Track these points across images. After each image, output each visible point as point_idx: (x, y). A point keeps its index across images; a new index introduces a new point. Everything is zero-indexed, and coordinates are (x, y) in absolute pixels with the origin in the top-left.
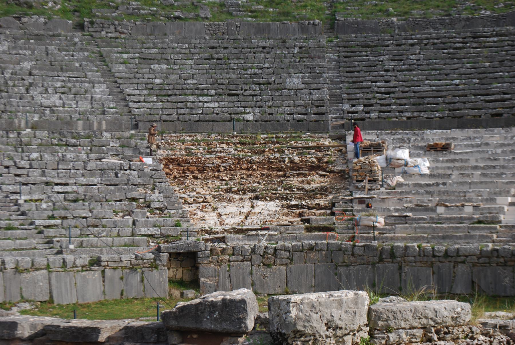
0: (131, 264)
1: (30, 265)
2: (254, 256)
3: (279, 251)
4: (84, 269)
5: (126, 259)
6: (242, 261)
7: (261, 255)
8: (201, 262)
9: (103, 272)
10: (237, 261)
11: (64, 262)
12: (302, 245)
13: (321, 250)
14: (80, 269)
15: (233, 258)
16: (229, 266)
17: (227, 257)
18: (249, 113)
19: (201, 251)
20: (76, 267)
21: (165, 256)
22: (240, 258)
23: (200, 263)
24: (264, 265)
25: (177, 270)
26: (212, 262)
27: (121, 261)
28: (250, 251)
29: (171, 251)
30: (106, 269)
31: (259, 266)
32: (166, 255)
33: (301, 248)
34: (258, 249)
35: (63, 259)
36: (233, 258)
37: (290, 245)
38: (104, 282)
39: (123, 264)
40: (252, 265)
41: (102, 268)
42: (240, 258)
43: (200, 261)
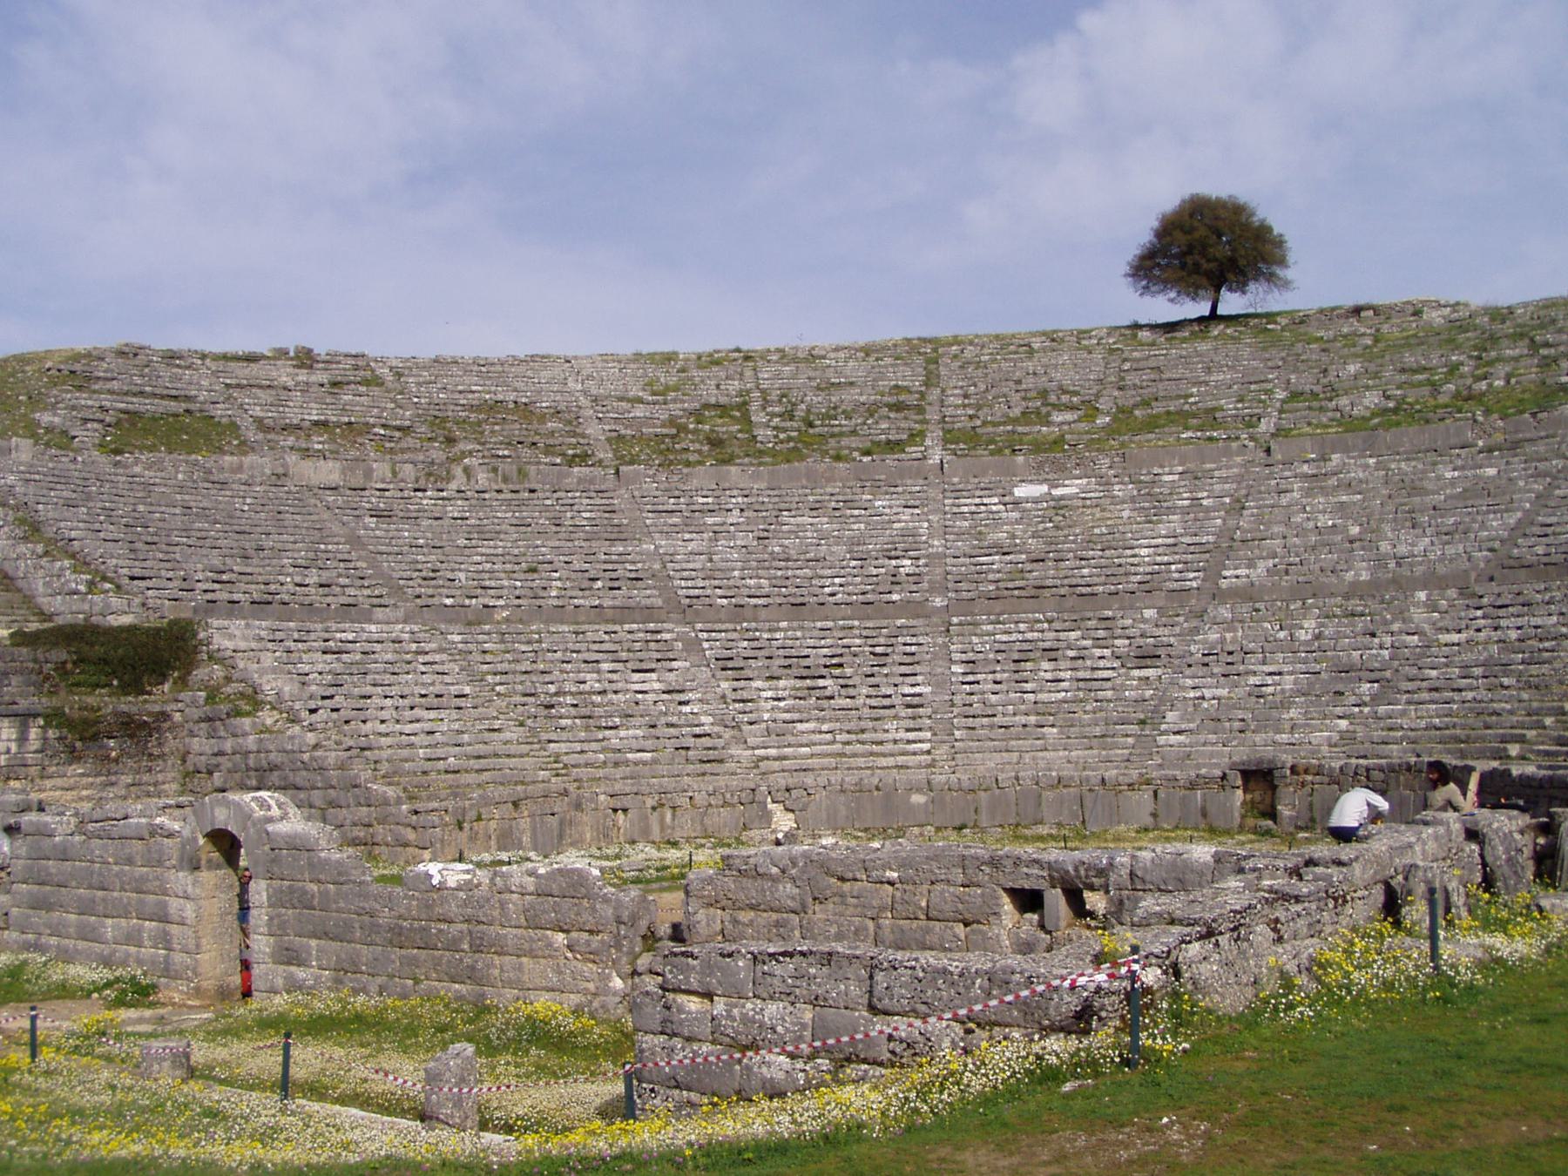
9: (1155, 793)
39: (1182, 783)
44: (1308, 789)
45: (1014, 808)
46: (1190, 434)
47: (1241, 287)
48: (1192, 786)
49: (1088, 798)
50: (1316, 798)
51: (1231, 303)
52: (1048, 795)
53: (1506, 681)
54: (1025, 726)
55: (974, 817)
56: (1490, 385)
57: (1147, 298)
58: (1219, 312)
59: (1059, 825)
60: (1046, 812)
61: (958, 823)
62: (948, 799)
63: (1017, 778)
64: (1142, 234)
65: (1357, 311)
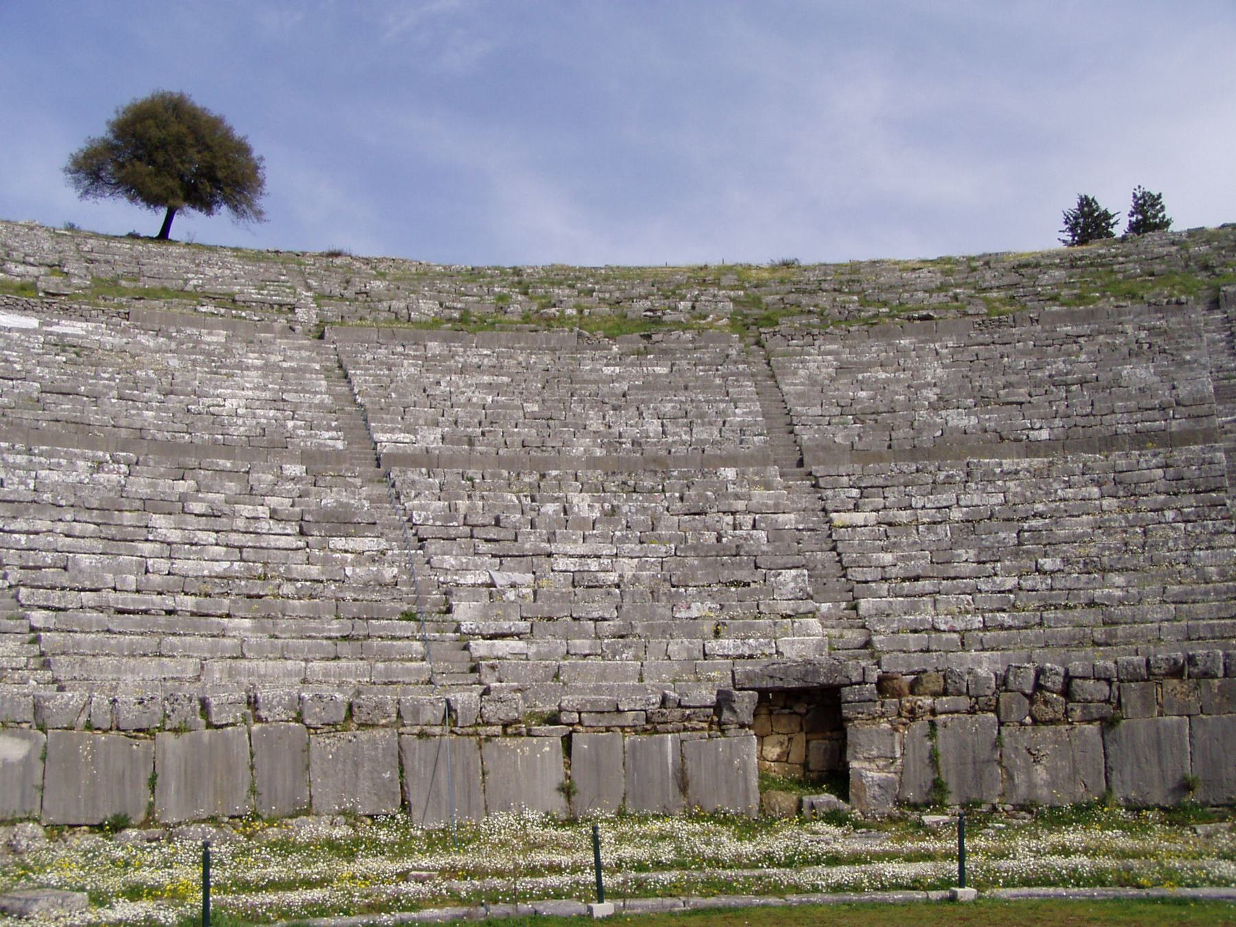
0: (648, 720)
1: (343, 713)
2: (1004, 697)
3: (1078, 681)
4: (509, 730)
5: (632, 706)
6: (972, 711)
7: (1025, 695)
8: (851, 715)
9: (567, 741)
10: (957, 712)
11: (450, 709)
12: (1148, 662)
13: (1207, 675)
14: (498, 729)
15: (945, 702)
16: (933, 724)
17: (927, 701)
18: (1041, 428)
19: (852, 684)
20: (488, 724)
21: (746, 702)
22: (964, 703)
23: (850, 720)
24: (1035, 721)
25: (790, 739)
26: (883, 715)
27: (618, 711)
28: (993, 685)
29: (764, 684)
30: (574, 731)
31: (1022, 724)
32: (750, 696)
33: (1143, 671)
34: (1016, 676)
35: (448, 701)
36: (942, 703)
37: (1110, 664)
38: (569, 766)
39: (629, 718)
40: (1001, 724)
41: (562, 729)
42: (964, 703)
43: (846, 712)
44: (920, 726)
45: (244, 776)
46: (211, 309)
47: (205, 204)
48: (652, 725)
49: (418, 755)
50: (944, 741)
51: (190, 224)
52: (324, 744)
53: (1047, 564)
54: (170, 612)
55: (145, 797)
56: (563, 312)
57: (91, 199)
58: (170, 237)
59: (351, 817)
60: (322, 789)
61: (105, 813)
62: (84, 750)
63: (253, 703)
64: (97, 128)
65: (337, 254)
